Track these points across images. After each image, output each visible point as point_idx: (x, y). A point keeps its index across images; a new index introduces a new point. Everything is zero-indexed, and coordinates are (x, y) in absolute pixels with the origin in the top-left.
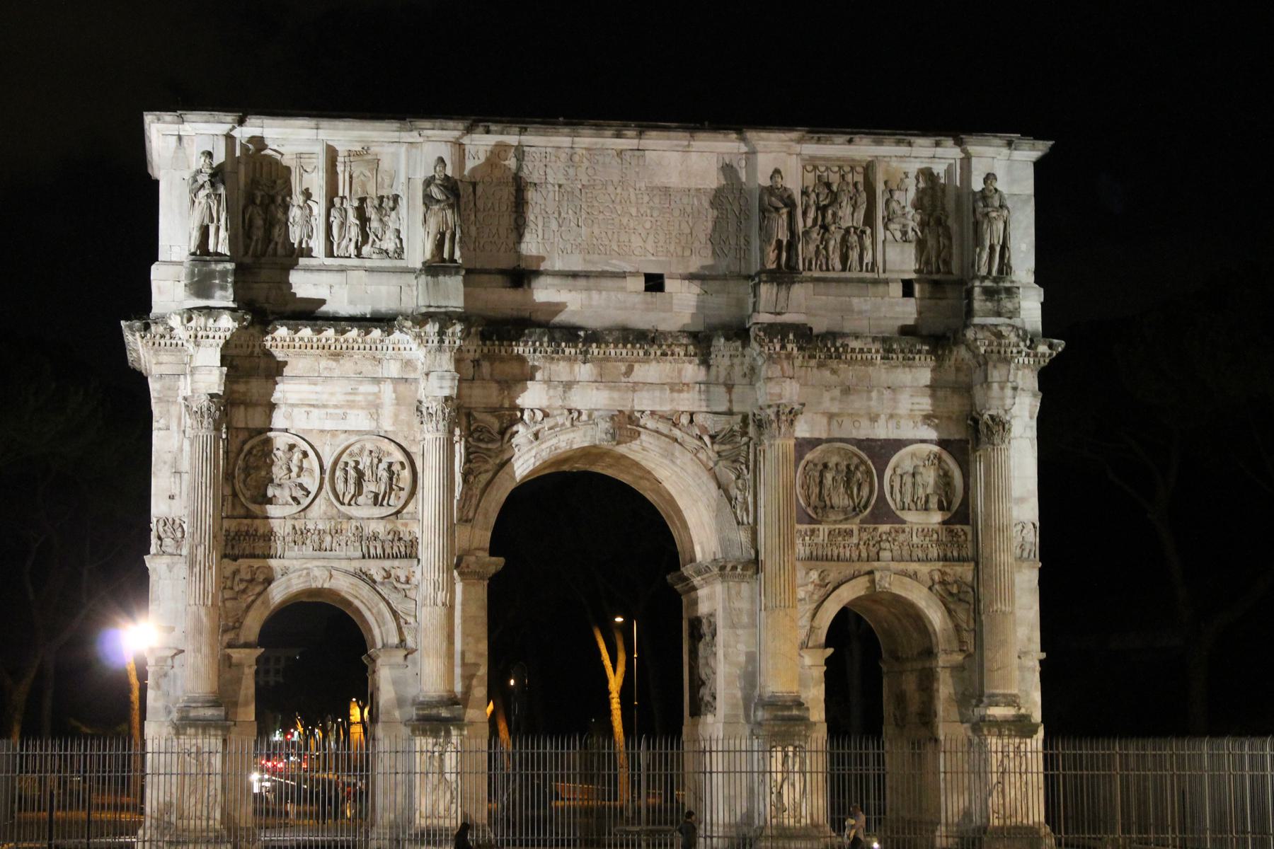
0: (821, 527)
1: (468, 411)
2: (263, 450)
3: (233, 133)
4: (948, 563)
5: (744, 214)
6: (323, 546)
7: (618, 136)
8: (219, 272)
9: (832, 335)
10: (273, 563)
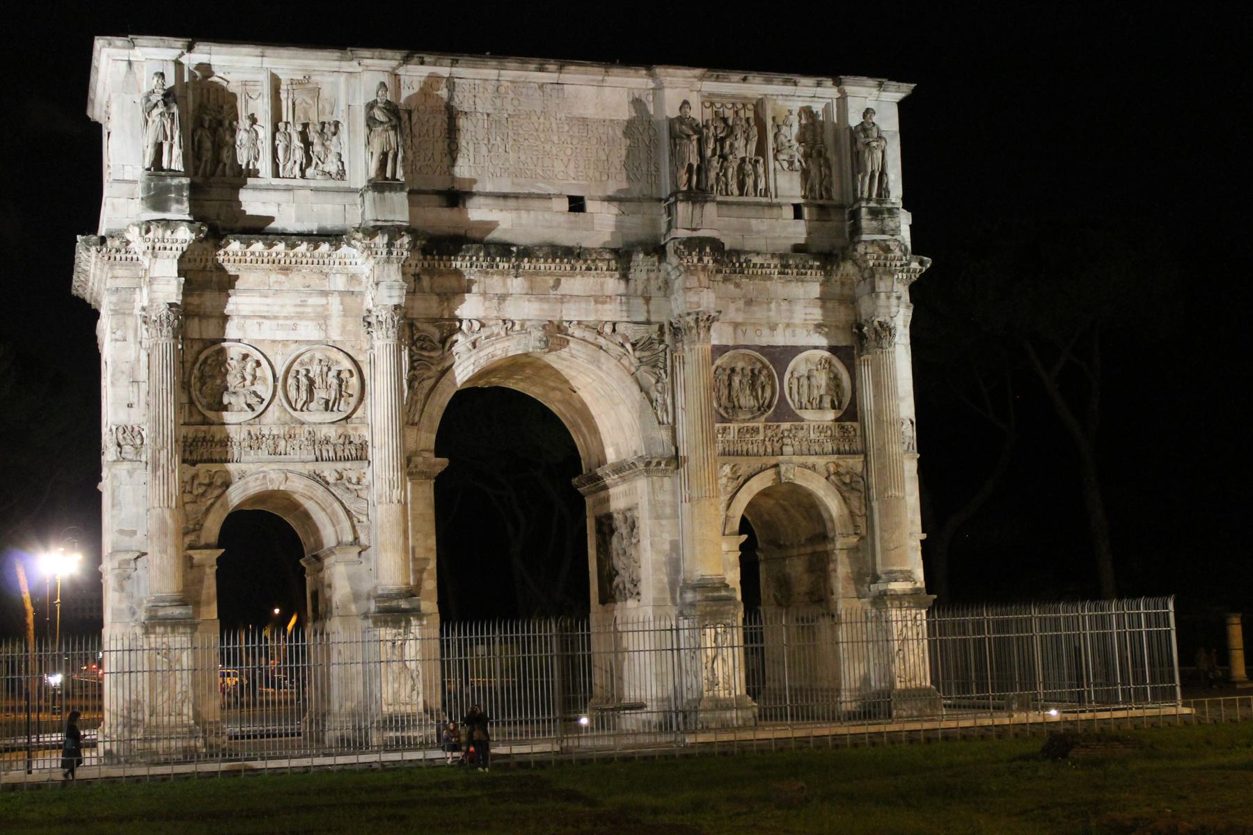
0: (731, 425)
1: (410, 321)
2: (217, 360)
3: (181, 60)
4: (842, 456)
5: (654, 143)
6: (278, 450)
7: (541, 70)
8: (176, 186)
9: (738, 253)
10: (231, 467)
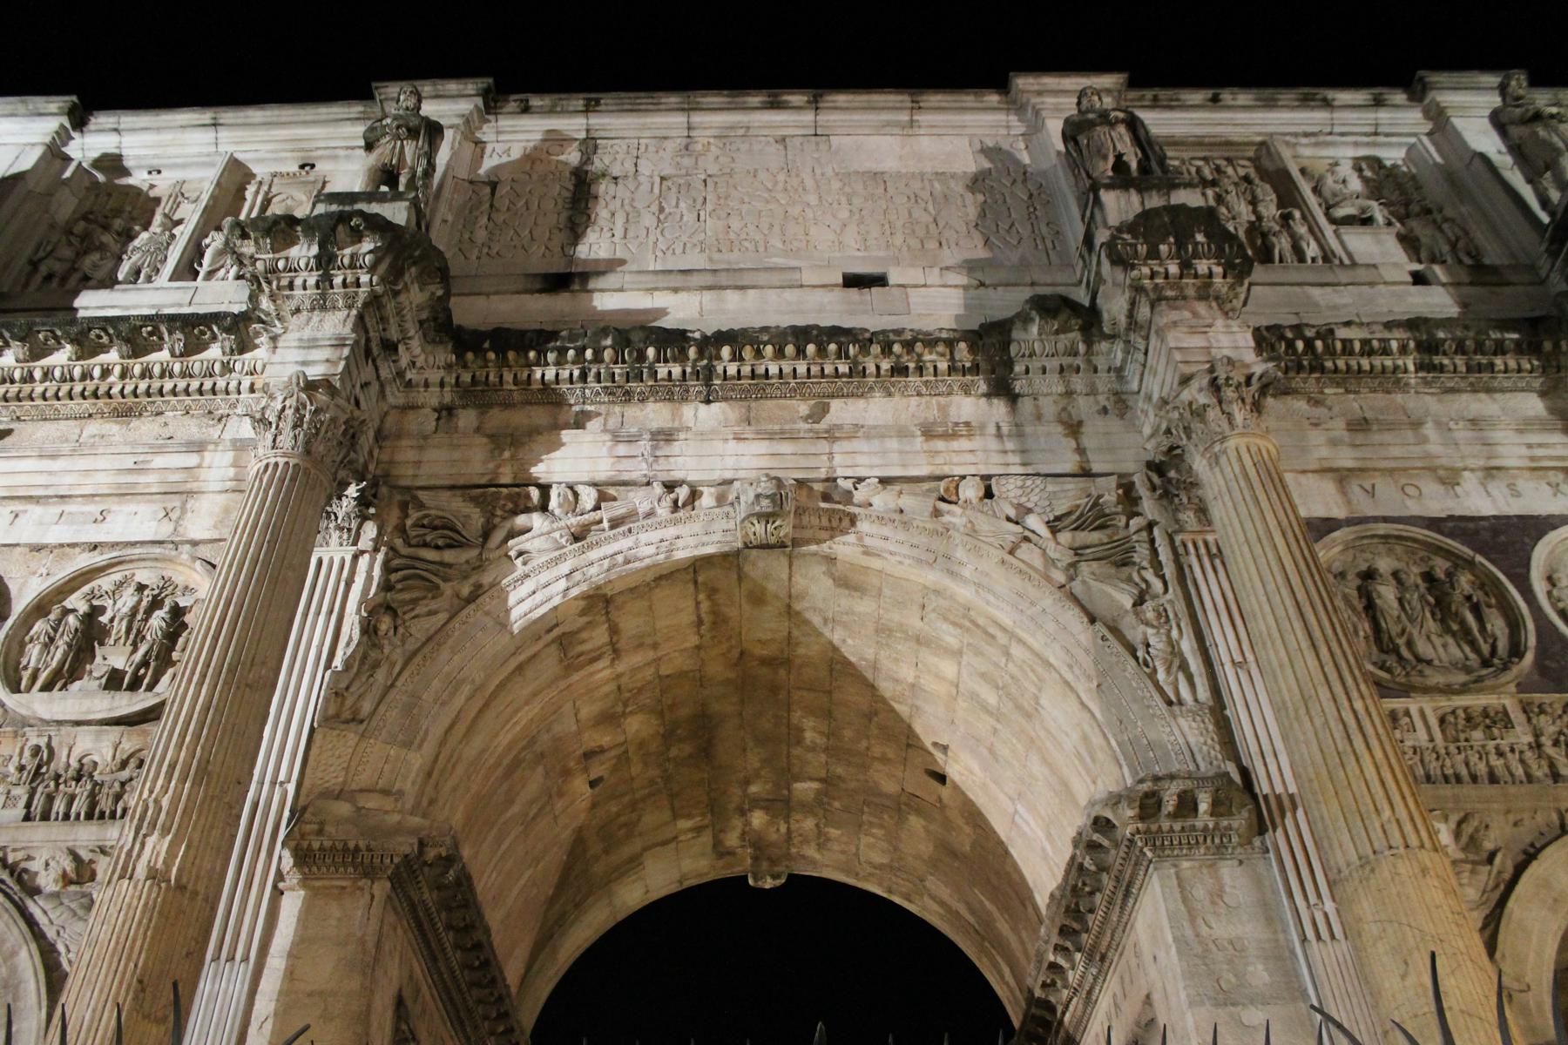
0: (1413, 705)
7: (775, 105)
